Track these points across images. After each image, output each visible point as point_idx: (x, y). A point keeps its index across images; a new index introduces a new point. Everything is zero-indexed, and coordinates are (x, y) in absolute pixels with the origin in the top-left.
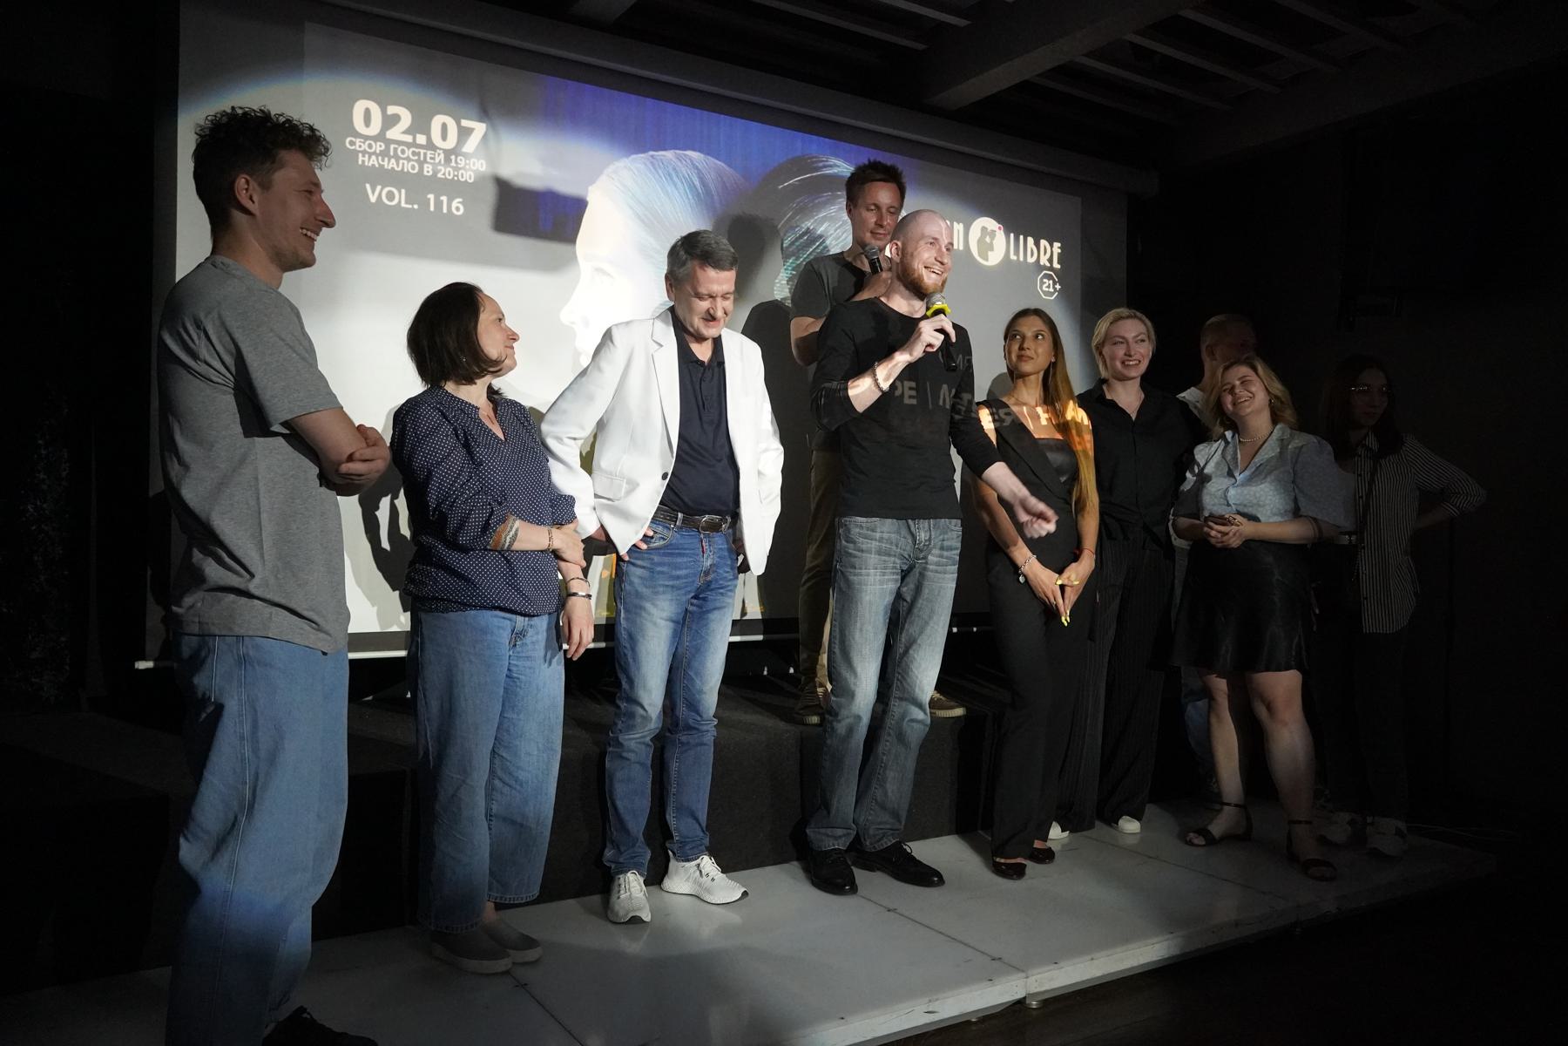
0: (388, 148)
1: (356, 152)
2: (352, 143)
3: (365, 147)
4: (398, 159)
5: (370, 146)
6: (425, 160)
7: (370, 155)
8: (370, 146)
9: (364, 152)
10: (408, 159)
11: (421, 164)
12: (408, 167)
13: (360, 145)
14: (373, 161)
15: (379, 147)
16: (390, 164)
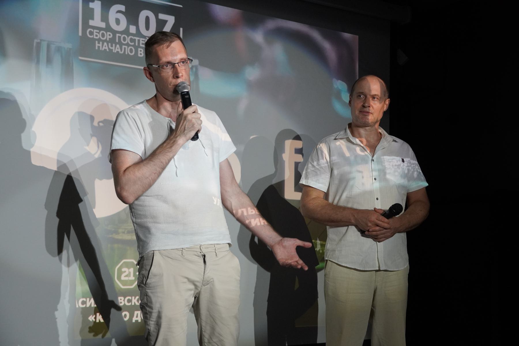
0: (114, 36)
1: (94, 40)
2: (91, 33)
3: (99, 36)
4: (121, 45)
5: (103, 35)
6: (139, 46)
7: (103, 41)
8: (103, 35)
9: (99, 40)
10: (128, 45)
11: (136, 48)
12: (128, 51)
13: (97, 35)
14: (105, 47)
15: (108, 36)
16: (116, 49)
